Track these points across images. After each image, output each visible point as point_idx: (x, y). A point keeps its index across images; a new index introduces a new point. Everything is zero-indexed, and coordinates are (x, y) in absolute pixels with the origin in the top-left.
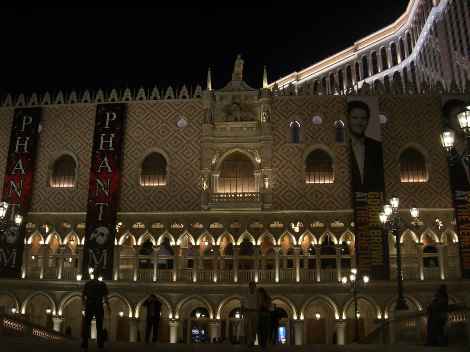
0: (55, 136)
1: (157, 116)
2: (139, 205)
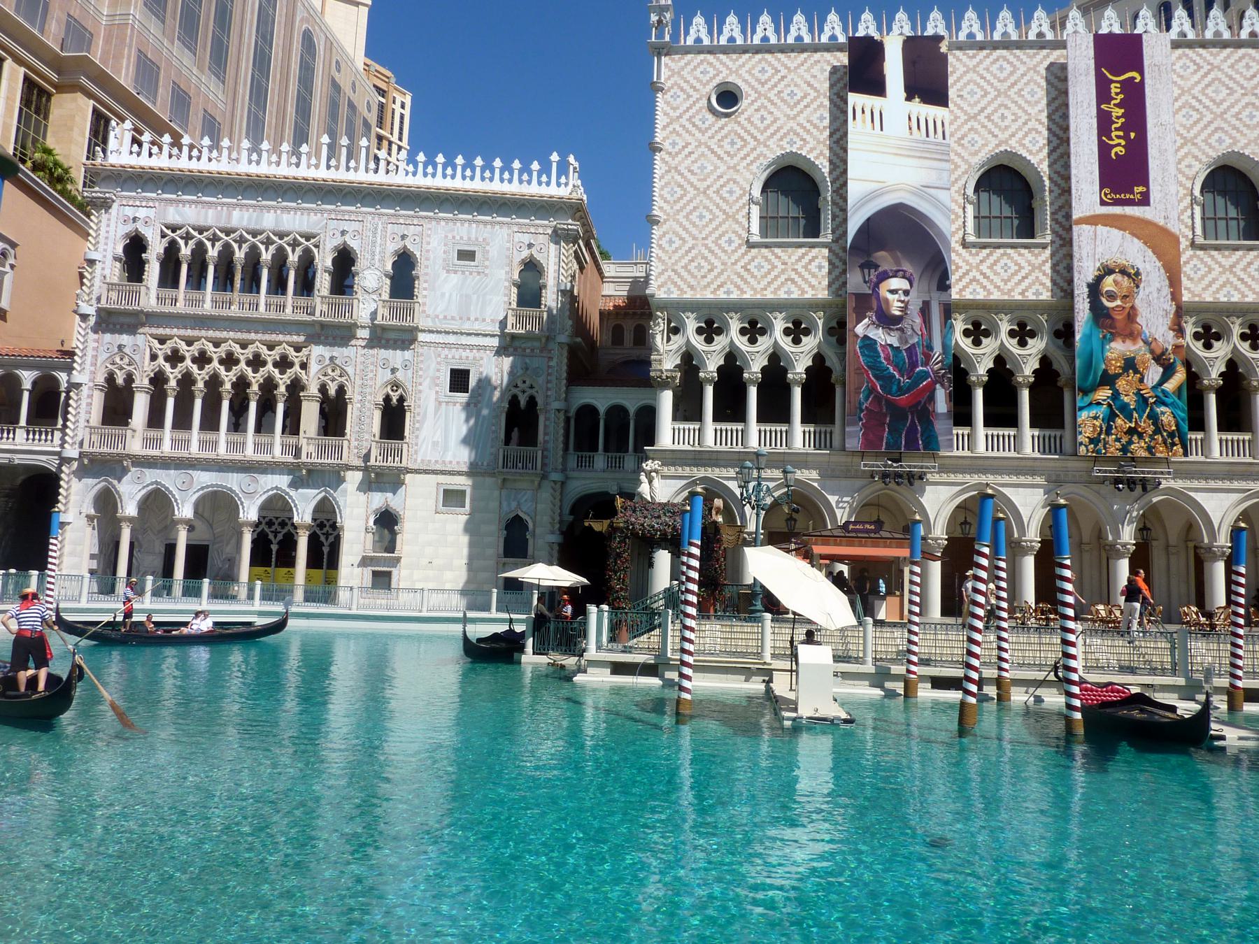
0: (975, 117)
1: (1231, 78)
2: (1210, 285)
